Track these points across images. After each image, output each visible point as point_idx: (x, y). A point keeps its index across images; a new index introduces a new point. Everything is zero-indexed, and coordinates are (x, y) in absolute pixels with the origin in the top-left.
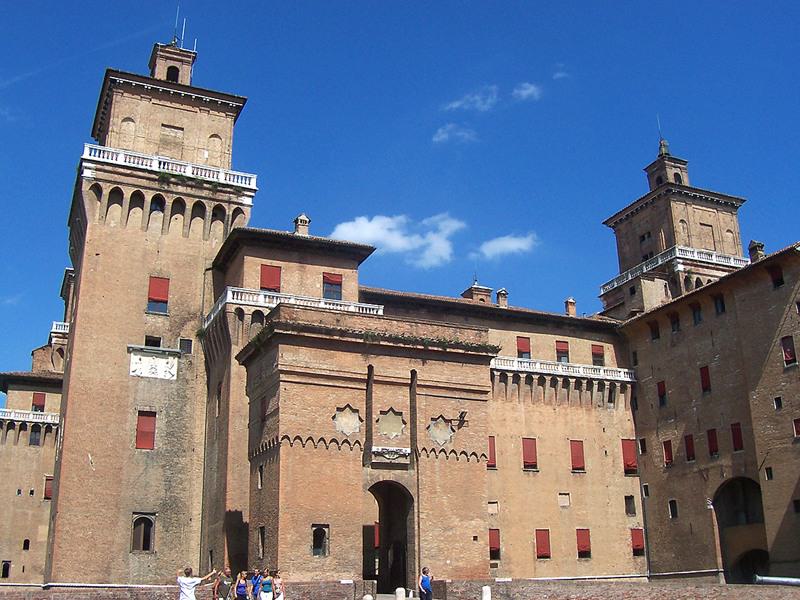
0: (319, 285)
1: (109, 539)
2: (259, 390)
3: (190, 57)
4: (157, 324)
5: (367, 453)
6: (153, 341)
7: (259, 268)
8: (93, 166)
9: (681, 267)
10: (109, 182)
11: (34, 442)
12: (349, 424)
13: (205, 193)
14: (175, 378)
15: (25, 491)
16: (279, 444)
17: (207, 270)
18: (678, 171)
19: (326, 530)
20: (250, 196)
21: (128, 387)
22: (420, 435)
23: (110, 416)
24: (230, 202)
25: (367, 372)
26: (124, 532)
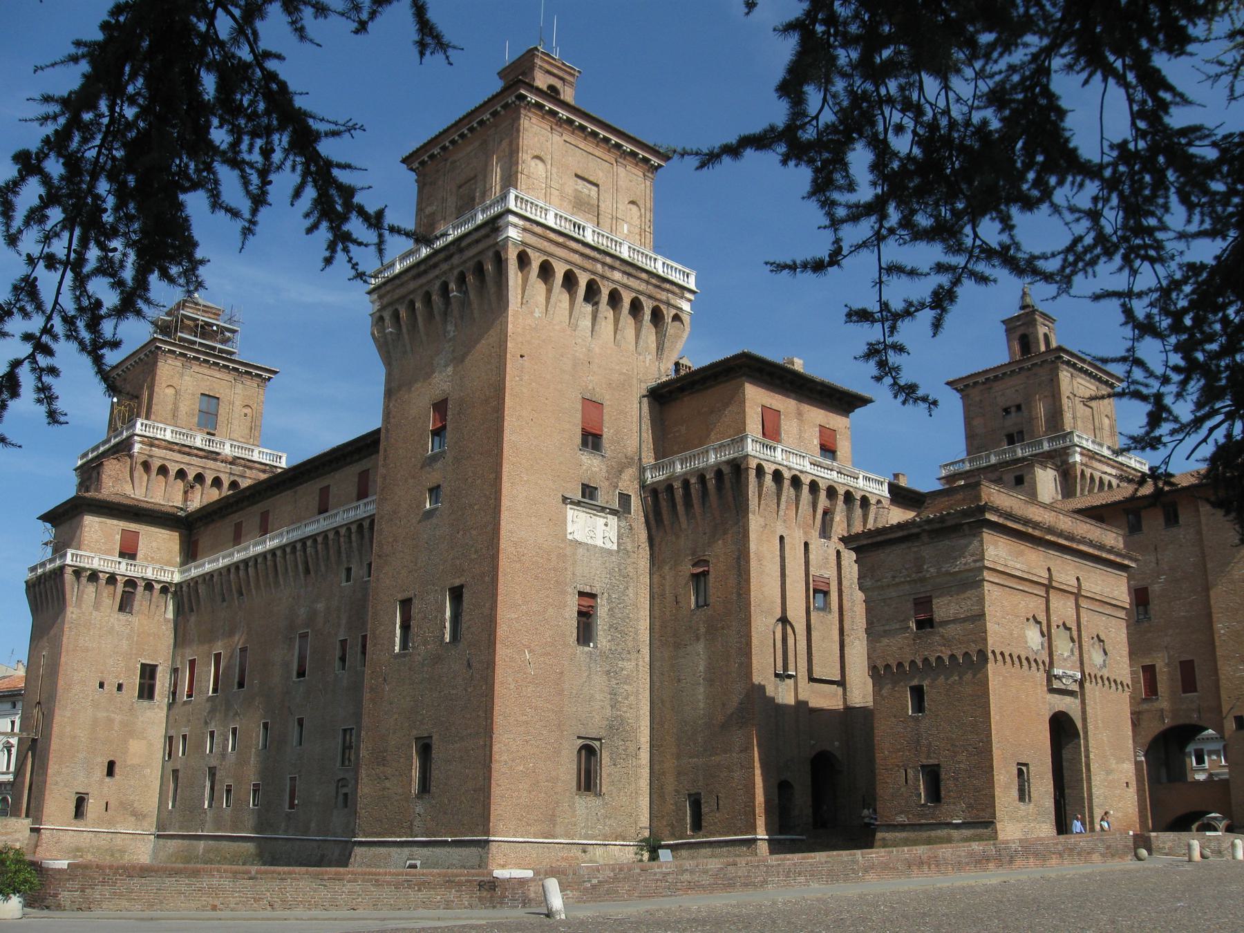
1: (554, 774)
3: (573, 75)
4: (592, 466)
5: (1050, 677)
6: (589, 491)
8: (521, 223)
9: (1078, 458)
10: (539, 250)
11: (125, 605)
12: (1034, 638)
13: (642, 287)
14: (615, 547)
15: (110, 687)
16: (986, 660)
17: (644, 396)
18: (1046, 330)
19: (1024, 769)
20: (689, 300)
21: (565, 555)
22: (1086, 656)
24: (669, 304)
25: (1047, 576)
26: (567, 768)
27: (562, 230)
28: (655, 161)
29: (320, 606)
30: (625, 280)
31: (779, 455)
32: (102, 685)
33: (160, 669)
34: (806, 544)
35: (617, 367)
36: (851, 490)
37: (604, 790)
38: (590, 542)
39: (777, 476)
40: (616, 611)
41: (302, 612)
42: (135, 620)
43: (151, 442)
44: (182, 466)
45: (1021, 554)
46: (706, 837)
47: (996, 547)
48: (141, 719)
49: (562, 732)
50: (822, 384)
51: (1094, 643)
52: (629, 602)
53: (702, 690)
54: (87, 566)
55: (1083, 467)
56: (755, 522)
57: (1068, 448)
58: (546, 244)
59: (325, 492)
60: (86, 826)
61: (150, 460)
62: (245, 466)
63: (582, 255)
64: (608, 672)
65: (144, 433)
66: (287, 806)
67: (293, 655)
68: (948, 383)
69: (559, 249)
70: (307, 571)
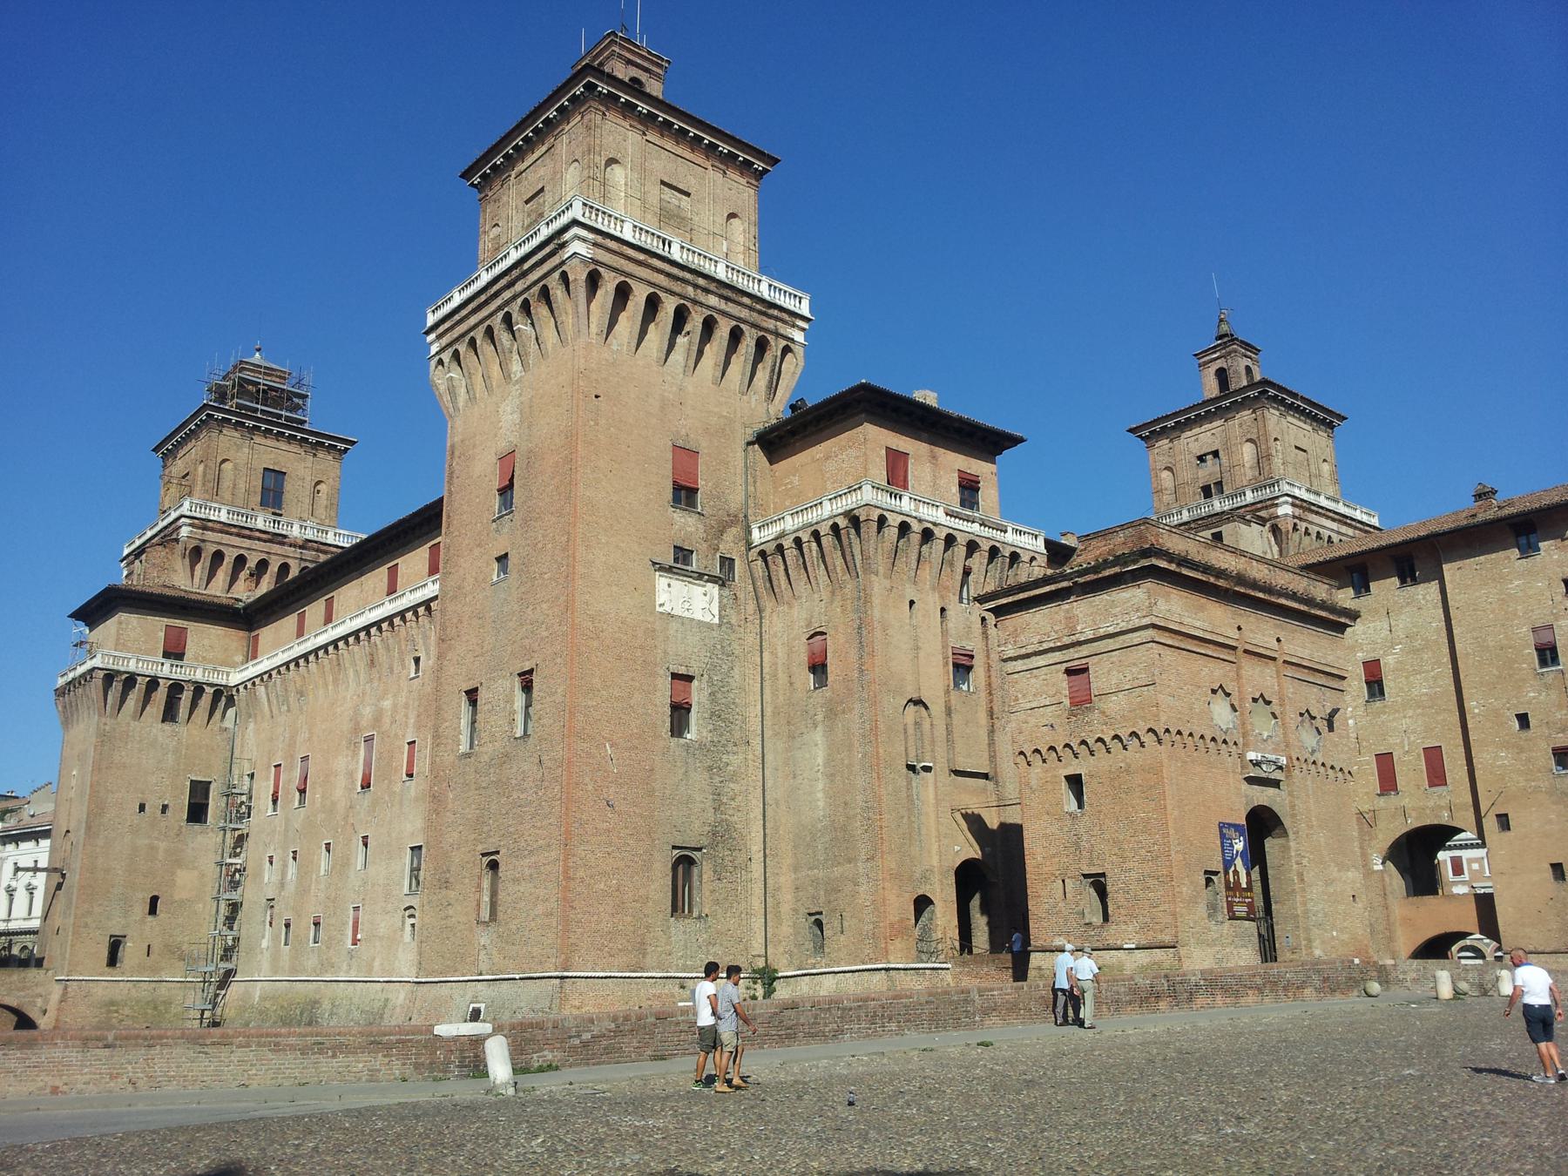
0: (955, 489)
1: (642, 892)
2: (1057, 656)
4: (686, 525)
7: (884, 452)
8: (591, 236)
10: (615, 270)
11: (169, 714)
13: (744, 314)
14: (716, 620)
17: (749, 444)
18: (1249, 362)
20: (803, 330)
21: (654, 631)
22: (1292, 737)
24: (777, 335)
27: (642, 244)
28: (759, 165)
29: (387, 704)
30: (722, 305)
31: (906, 505)
33: (212, 787)
34: (943, 610)
35: (716, 410)
36: (998, 545)
37: (706, 911)
38: (686, 614)
39: (904, 528)
40: (719, 696)
41: (367, 712)
43: (204, 524)
44: (242, 552)
45: (1202, 608)
46: (828, 965)
47: (1167, 597)
49: (653, 840)
50: (960, 420)
51: (1302, 722)
52: (734, 685)
53: (820, 786)
55: (1296, 520)
56: (878, 585)
57: (1277, 498)
58: (623, 261)
59: (393, 572)
61: (202, 545)
62: (318, 550)
63: (668, 275)
64: (710, 768)
65: (193, 514)
66: (350, 941)
67: (357, 762)
68: (1131, 431)
69: (639, 268)
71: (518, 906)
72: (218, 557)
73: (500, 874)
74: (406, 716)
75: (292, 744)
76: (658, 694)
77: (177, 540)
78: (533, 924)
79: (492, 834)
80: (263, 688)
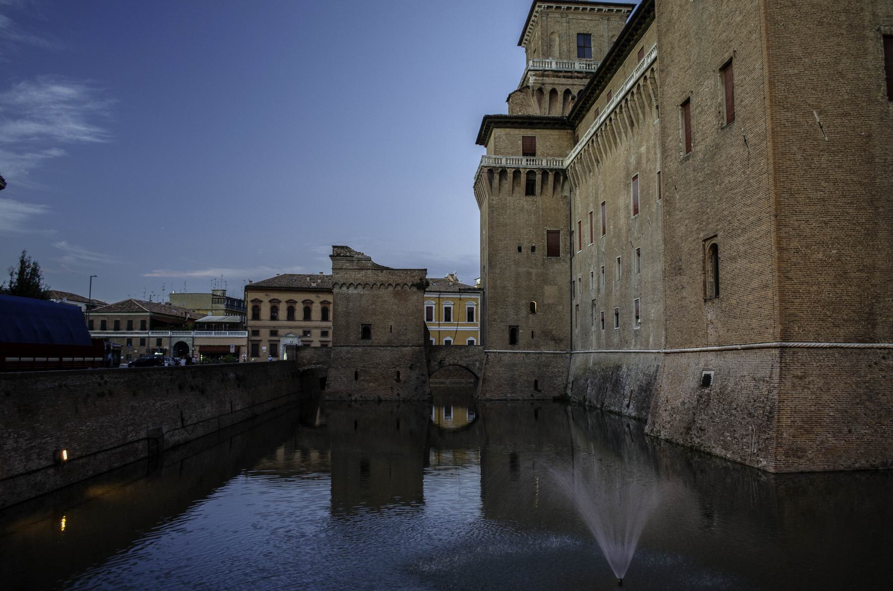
11: (530, 190)
23: (838, 44)
29: (643, 149)
32: (520, 249)
33: (562, 232)
41: (633, 160)
42: (538, 199)
43: (543, 73)
44: (568, 87)
48: (551, 270)
49: (877, 208)
54: (498, 166)
60: (519, 349)
70: (632, 124)
71: (737, 282)
72: (553, 92)
73: (719, 256)
74: (655, 154)
75: (597, 197)
76: (870, 57)
77: (528, 87)
78: (751, 297)
79: (710, 221)
80: (580, 166)
